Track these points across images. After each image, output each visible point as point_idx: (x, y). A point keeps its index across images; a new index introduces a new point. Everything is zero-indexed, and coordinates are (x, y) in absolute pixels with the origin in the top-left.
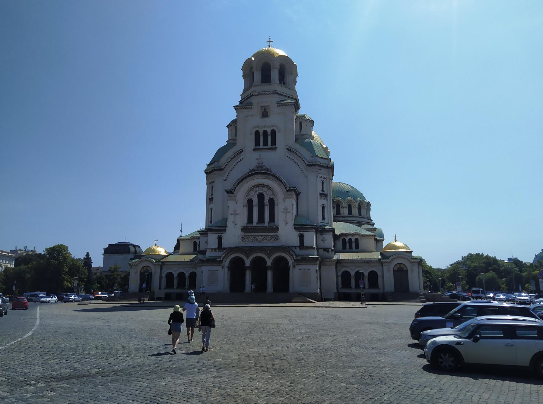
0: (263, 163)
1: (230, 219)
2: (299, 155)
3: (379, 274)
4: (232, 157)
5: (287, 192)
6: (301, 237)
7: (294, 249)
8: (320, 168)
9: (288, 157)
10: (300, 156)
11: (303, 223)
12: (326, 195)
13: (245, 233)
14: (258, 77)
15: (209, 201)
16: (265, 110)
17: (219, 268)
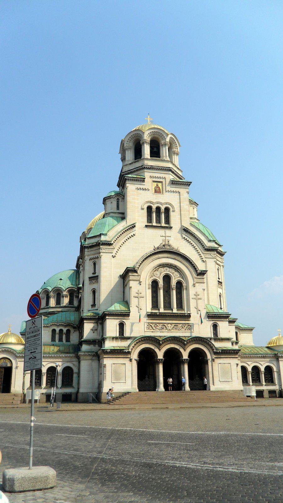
0: (169, 242)
1: (134, 302)
2: (197, 238)
3: (275, 369)
4: (122, 232)
5: (197, 276)
6: (215, 327)
7: (209, 339)
8: (217, 255)
9: (184, 238)
10: (198, 239)
11: (215, 312)
12: (221, 283)
13: (151, 320)
14: (147, 150)
15: (89, 280)
16: (157, 185)
17: (126, 361)
